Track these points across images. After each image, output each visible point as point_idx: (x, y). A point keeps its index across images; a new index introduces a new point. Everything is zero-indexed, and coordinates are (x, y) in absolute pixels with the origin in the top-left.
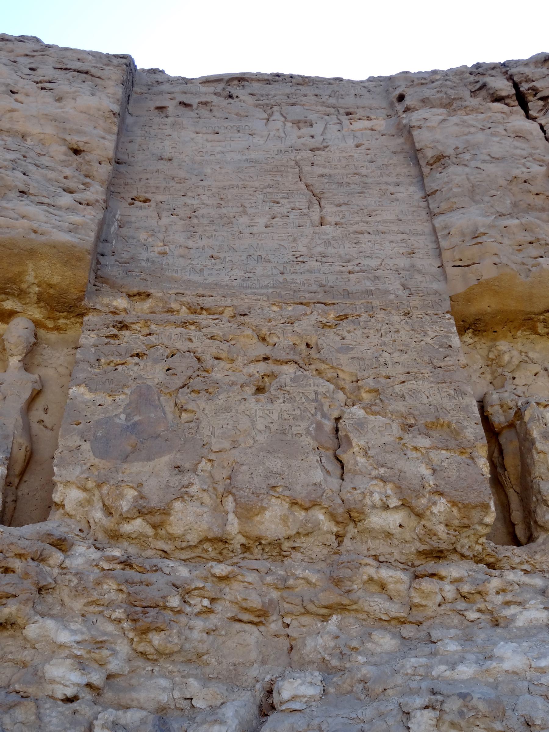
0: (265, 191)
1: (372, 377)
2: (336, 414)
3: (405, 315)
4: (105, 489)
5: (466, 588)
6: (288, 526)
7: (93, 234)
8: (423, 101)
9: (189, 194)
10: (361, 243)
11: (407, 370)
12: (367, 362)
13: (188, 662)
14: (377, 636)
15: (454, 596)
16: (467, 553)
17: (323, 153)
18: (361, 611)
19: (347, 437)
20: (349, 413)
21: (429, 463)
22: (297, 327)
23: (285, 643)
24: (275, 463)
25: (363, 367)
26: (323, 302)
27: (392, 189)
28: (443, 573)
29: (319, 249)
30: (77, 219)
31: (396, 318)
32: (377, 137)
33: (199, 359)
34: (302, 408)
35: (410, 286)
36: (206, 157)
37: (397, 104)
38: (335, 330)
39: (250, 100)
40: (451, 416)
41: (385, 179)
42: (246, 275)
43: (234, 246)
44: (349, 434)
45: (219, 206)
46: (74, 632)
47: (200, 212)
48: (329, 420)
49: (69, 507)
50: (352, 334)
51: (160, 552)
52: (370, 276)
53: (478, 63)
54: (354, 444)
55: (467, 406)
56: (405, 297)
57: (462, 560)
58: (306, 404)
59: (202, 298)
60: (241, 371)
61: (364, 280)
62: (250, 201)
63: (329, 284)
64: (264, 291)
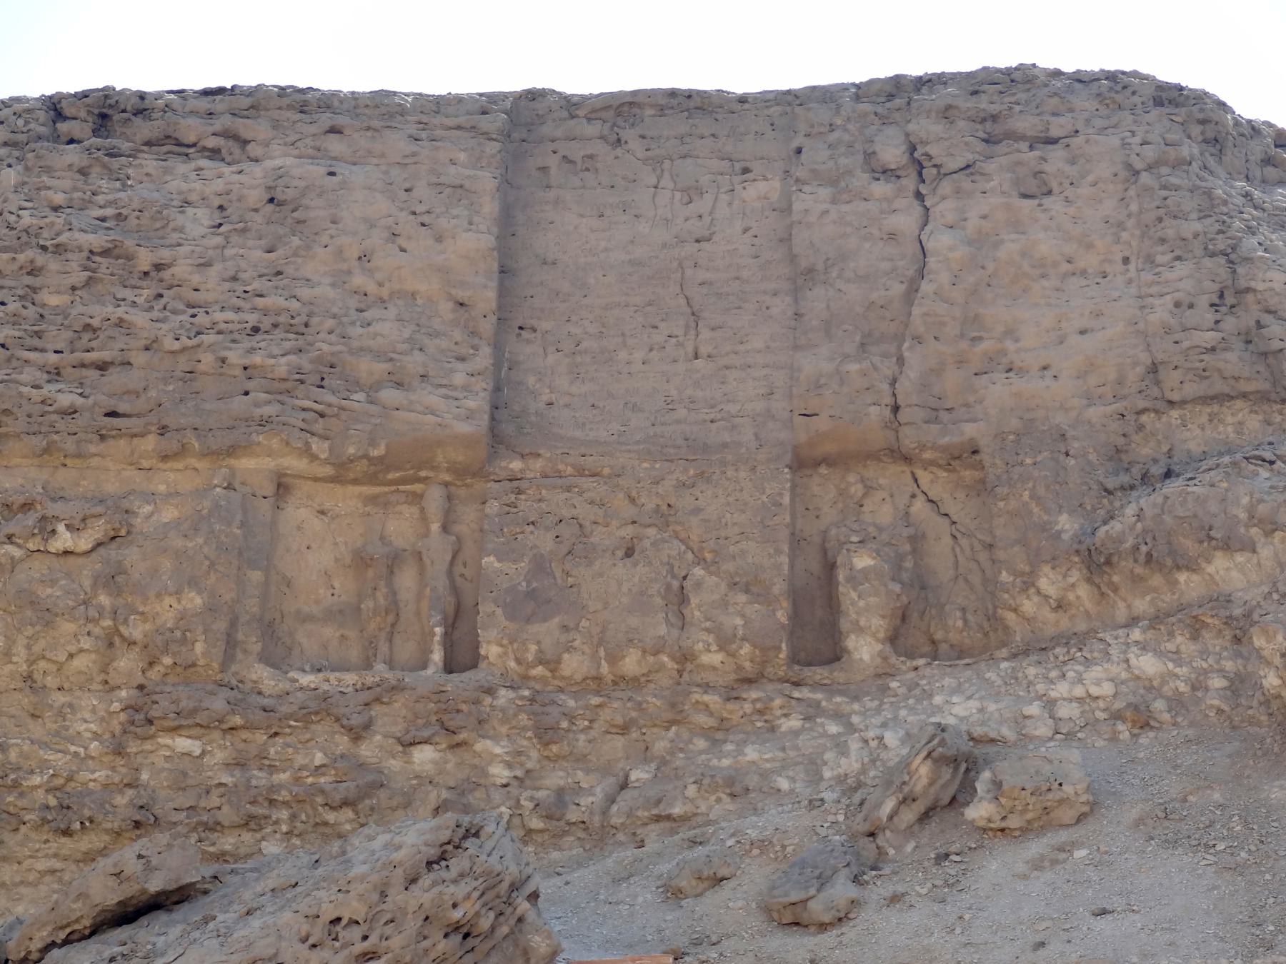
2: (683, 574)
4: (515, 646)
5: (759, 706)
7: (486, 417)
9: (574, 318)
13: (577, 760)
14: (695, 741)
18: (689, 723)
23: (642, 745)
24: (634, 621)
28: (745, 696)
29: (689, 392)
30: (471, 404)
31: (743, 474)
33: (581, 526)
42: (622, 429)
46: (503, 747)
47: (584, 345)
49: (491, 659)
53: (897, 76)
64: (636, 448)
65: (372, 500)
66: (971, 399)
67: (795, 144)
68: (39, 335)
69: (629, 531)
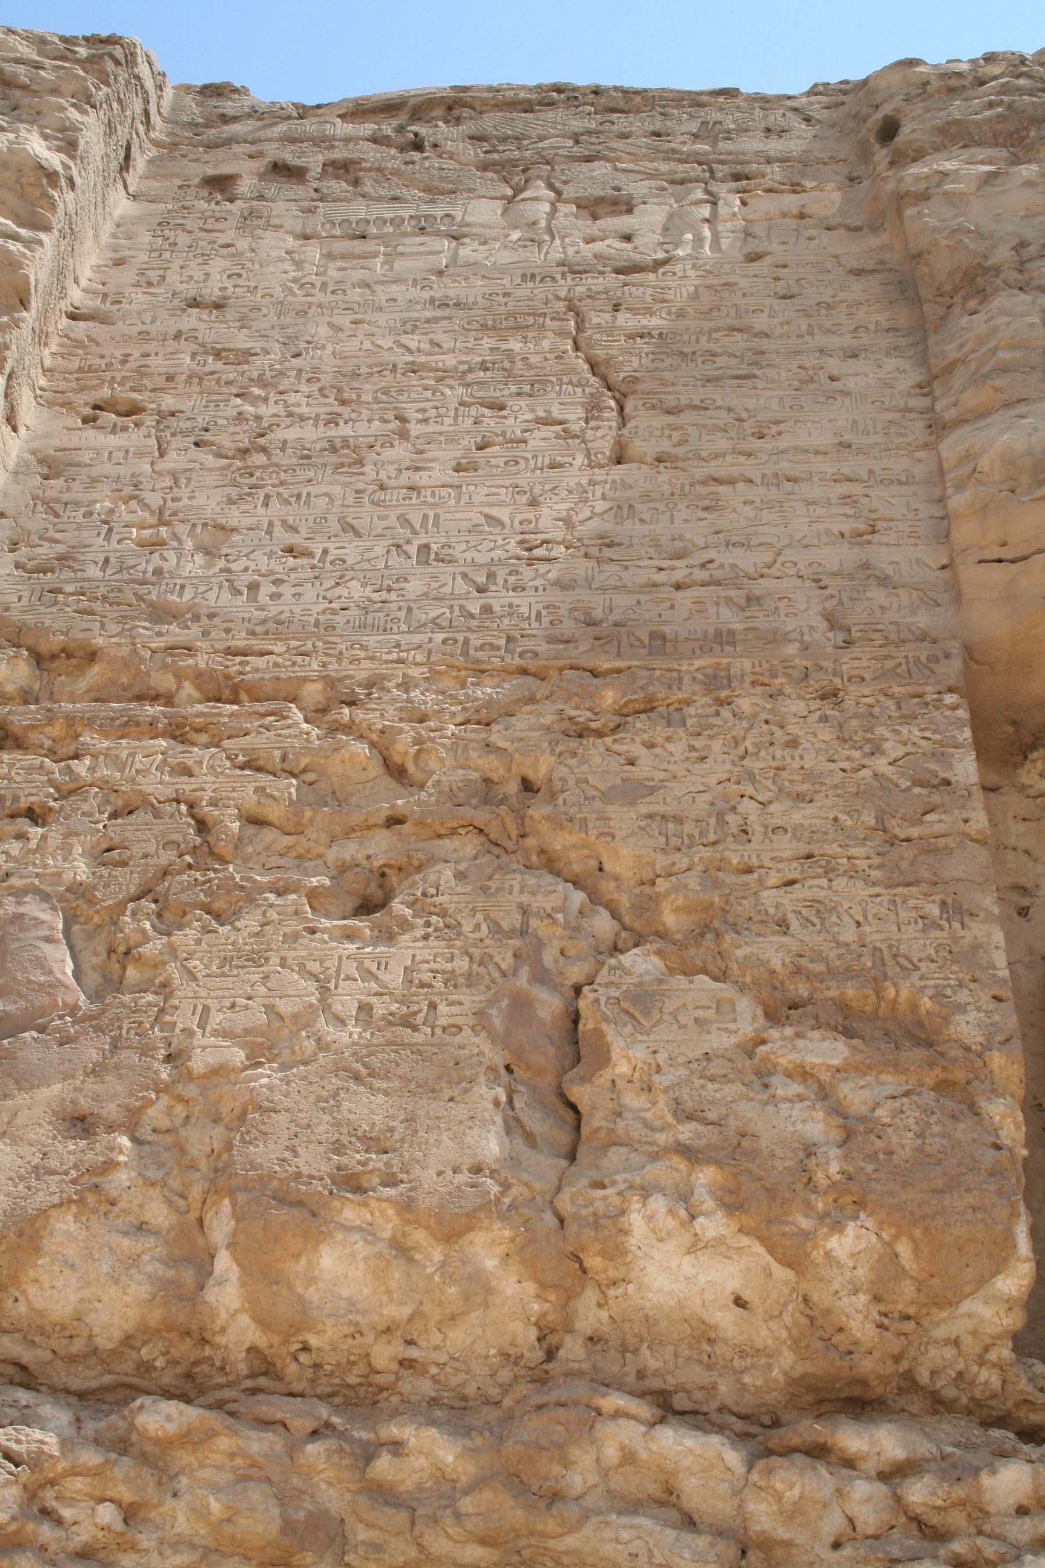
0: (470, 377)
1: (700, 868)
2: (576, 973)
3: (823, 697)
5: (919, 1493)
6: (388, 1292)
8: (942, 131)
10: (724, 508)
11: (804, 848)
12: (689, 828)
15: (886, 1516)
16: (950, 1393)
17: (651, 276)
19: (599, 1033)
20: (612, 968)
21: (838, 1111)
22: (497, 736)
25: (675, 841)
26: (585, 665)
27: (833, 365)
32: (812, 232)
34: (476, 952)
35: (848, 622)
36: (319, 297)
37: (877, 147)
38: (608, 740)
39: (472, 153)
40: (921, 978)
41: (820, 340)
42: (376, 597)
43: (354, 522)
44: (604, 1026)
45: (333, 420)
48: (555, 988)
50: (657, 751)
51: (10, 1369)
52: (732, 593)
54: (614, 1056)
55: (976, 947)
56: (830, 650)
57: (936, 1412)
58: (488, 942)
59: (239, 659)
60: (320, 856)
61: (717, 604)
62: (422, 405)
63: (613, 618)
64: (417, 638)
69: (380, 847)
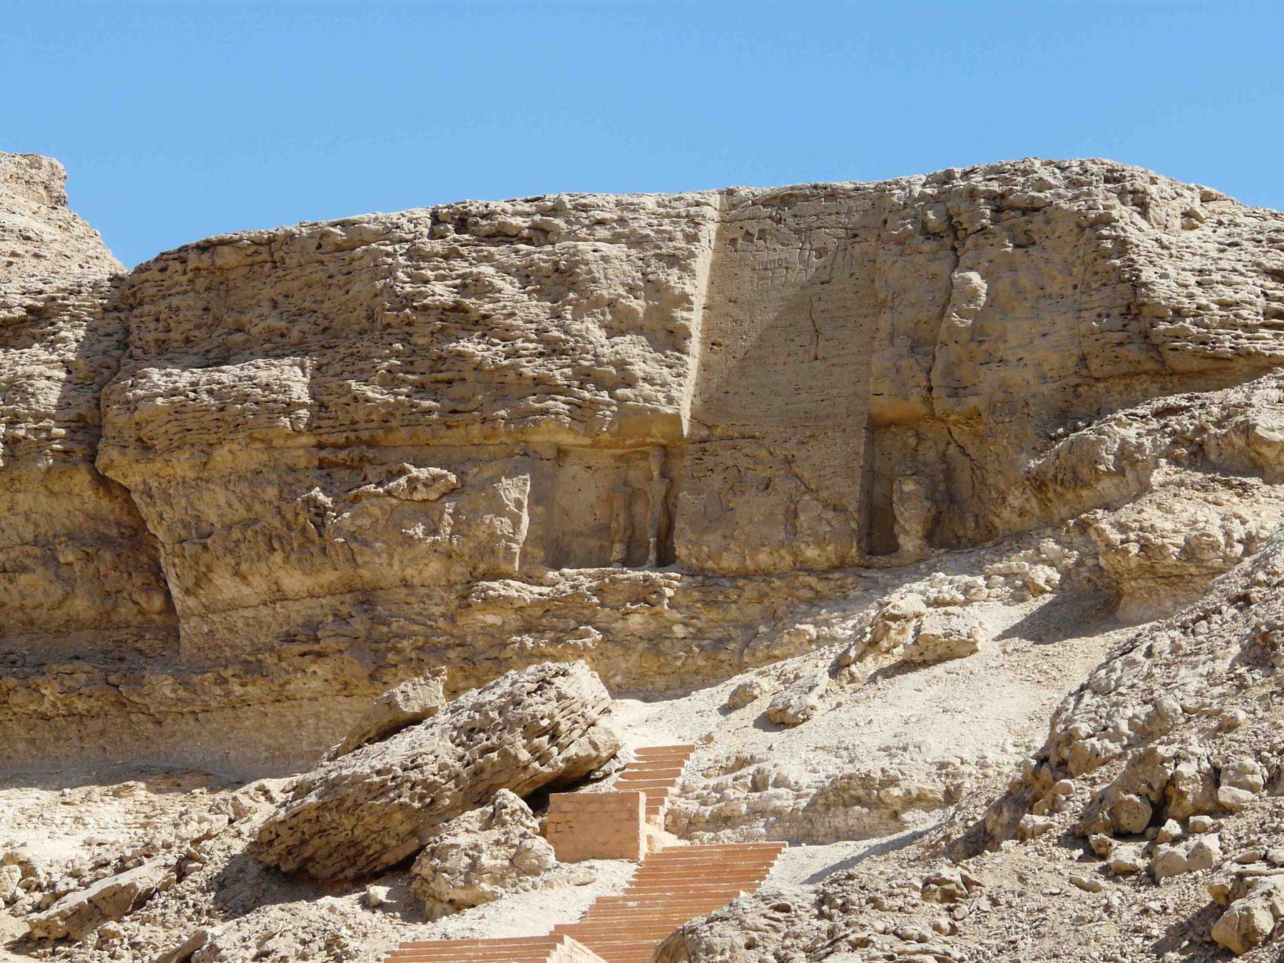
22: (788, 446)
65: (620, 458)
66: (977, 381)
67: (884, 217)
68: (412, 363)
69: (768, 473)
